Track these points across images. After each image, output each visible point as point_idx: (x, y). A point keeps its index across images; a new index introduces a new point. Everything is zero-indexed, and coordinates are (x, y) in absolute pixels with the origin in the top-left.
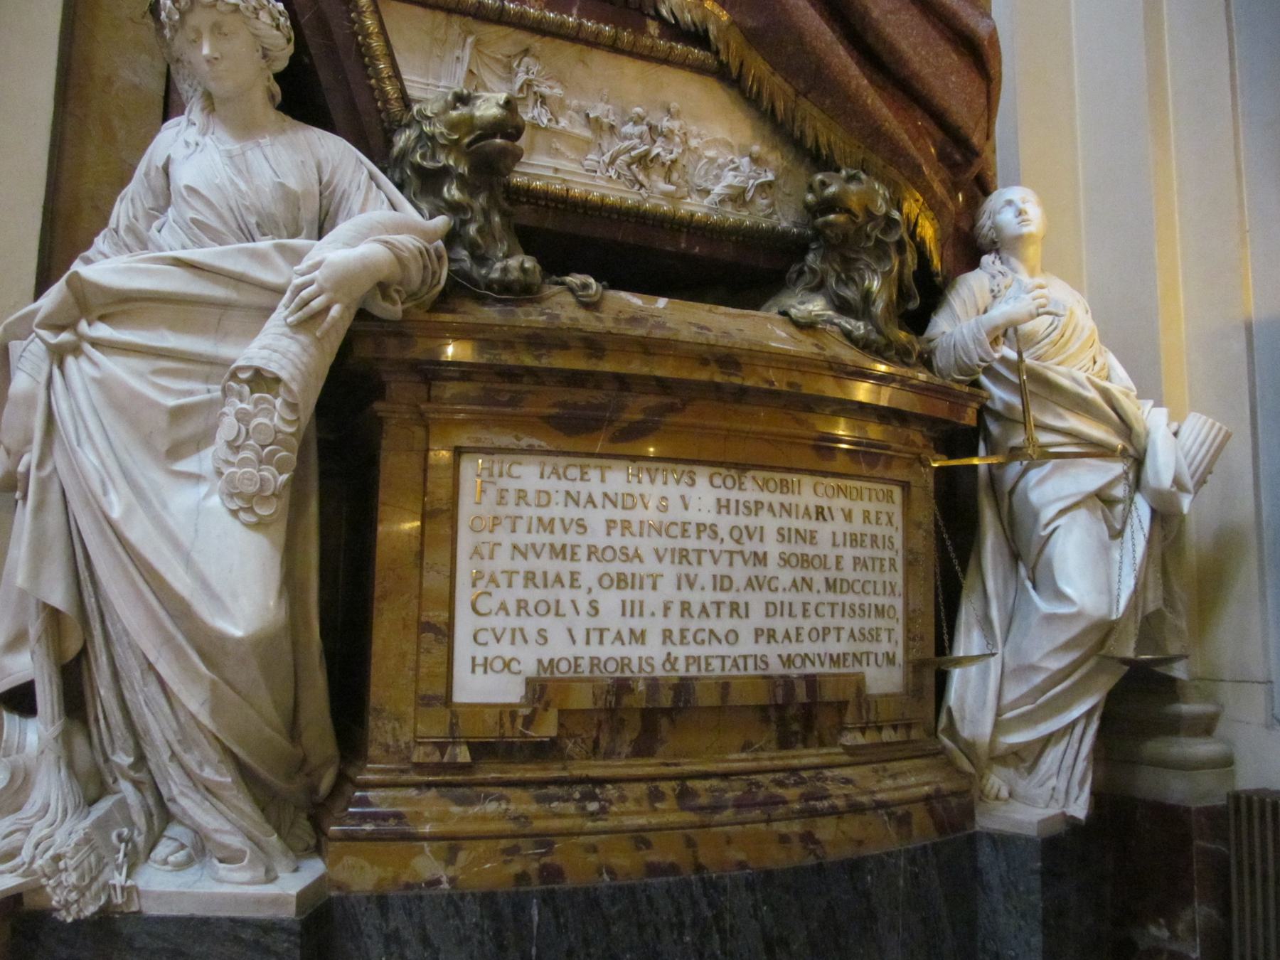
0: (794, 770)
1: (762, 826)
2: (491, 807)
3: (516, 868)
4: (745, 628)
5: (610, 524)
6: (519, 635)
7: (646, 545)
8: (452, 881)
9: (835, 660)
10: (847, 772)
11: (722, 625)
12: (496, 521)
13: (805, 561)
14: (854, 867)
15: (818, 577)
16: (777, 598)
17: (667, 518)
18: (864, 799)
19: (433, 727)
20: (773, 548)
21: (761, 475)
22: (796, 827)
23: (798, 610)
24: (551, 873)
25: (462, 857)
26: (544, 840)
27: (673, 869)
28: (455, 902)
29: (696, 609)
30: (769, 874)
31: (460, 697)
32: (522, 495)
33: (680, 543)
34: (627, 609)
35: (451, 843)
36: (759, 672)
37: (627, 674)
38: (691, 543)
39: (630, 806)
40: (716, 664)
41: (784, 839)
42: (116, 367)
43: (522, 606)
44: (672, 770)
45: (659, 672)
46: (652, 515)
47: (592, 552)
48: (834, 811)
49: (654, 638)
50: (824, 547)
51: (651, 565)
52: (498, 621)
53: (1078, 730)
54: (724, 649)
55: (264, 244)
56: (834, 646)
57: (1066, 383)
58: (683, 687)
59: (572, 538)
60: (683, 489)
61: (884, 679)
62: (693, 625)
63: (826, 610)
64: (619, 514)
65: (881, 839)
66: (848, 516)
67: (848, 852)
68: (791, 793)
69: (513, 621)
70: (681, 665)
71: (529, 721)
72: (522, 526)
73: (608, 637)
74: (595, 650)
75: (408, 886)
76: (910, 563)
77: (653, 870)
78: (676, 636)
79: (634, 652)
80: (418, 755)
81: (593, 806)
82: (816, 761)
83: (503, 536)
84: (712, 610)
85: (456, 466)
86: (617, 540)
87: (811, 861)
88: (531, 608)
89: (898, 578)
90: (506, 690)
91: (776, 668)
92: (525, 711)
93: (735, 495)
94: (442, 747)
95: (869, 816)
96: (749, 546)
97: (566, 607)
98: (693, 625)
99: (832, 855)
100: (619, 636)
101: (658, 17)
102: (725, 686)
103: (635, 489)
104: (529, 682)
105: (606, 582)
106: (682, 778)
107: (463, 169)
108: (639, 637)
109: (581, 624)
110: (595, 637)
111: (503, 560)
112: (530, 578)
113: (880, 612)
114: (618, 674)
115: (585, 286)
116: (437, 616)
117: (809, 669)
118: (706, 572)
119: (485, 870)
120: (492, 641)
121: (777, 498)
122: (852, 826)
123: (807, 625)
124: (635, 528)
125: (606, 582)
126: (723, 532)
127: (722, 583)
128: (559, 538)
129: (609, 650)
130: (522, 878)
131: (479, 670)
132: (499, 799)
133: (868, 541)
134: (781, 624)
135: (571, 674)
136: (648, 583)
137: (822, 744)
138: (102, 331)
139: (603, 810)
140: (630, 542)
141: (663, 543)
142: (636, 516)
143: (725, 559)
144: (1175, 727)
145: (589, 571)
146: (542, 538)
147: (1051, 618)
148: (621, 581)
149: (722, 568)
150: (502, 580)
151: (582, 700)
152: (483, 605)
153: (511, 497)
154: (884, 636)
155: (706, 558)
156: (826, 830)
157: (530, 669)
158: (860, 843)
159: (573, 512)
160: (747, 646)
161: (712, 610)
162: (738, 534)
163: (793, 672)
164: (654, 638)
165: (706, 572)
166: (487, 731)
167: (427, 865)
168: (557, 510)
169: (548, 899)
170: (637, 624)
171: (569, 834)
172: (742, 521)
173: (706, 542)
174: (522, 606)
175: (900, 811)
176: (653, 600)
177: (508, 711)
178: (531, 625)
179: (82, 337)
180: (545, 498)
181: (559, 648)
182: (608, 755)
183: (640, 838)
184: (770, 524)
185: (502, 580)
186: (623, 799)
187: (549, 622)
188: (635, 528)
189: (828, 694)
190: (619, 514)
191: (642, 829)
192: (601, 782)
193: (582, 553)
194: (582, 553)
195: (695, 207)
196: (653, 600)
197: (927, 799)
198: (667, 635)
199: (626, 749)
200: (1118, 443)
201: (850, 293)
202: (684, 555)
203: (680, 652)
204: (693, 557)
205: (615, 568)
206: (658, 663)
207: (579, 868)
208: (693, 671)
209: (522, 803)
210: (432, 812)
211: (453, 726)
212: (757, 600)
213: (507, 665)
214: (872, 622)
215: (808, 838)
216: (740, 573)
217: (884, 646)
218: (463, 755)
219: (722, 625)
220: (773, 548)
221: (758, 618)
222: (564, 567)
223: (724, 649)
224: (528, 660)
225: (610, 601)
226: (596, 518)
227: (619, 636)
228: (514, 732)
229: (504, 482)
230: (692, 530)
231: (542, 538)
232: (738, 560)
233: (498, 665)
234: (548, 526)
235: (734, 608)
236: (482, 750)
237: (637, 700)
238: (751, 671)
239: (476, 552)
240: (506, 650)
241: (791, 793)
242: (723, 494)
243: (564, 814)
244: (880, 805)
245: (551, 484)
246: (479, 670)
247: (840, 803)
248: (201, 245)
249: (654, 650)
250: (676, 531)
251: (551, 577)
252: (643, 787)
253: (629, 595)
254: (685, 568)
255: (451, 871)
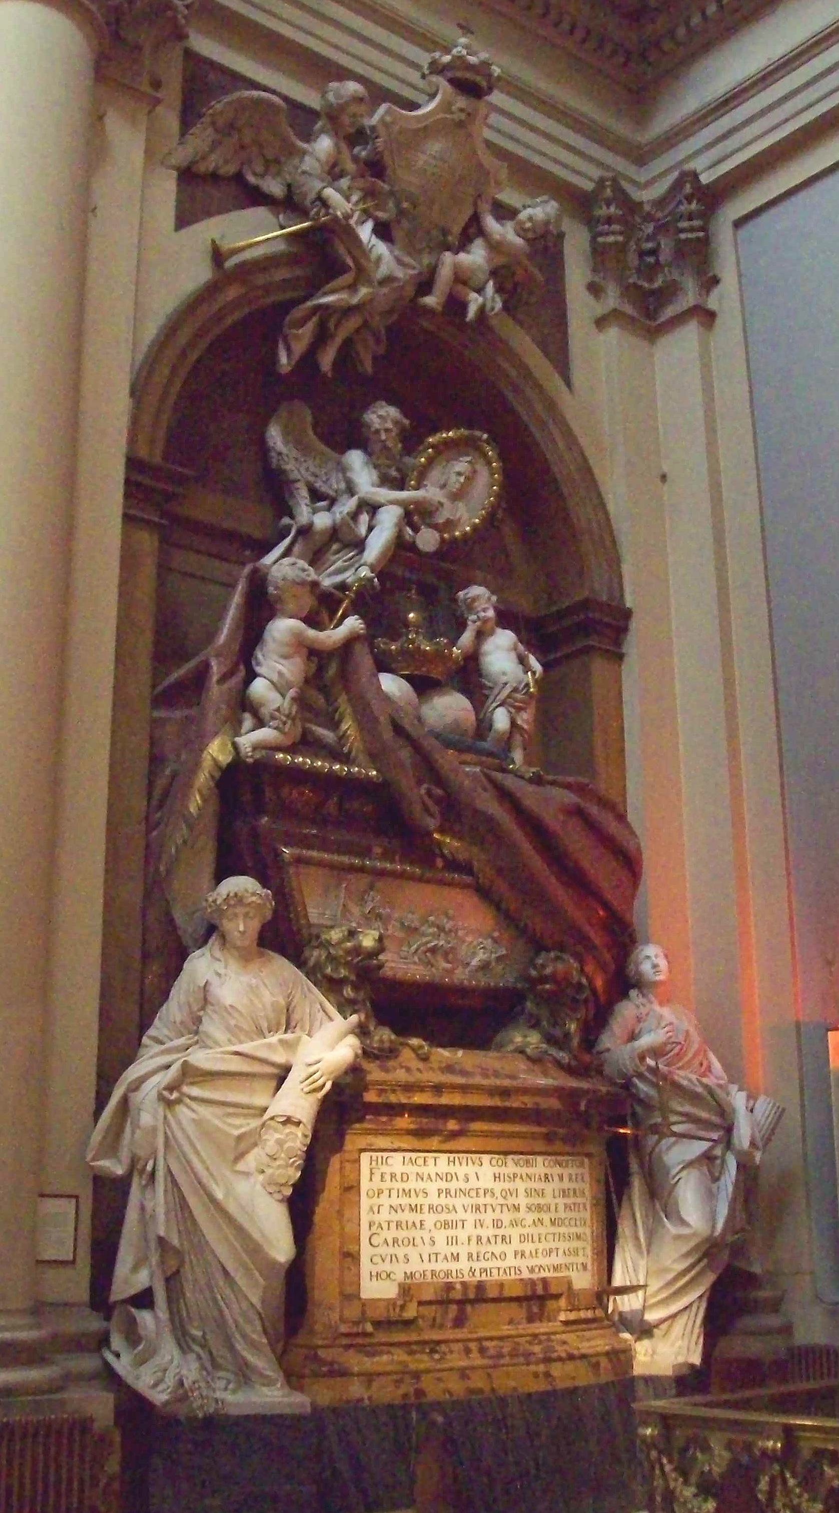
0: (535, 1336)
1: (524, 1368)
2: (385, 1358)
3: (401, 1392)
4: (509, 1250)
5: (440, 1192)
6: (394, 1258)
7: (459, 1202)
8: (370, 1398)
9: (556, 1268)
10: (564, 1337)
11: (498, 1249)
12: (380, 1192)
13: (539, 1208)
14: (574, 1391)
15: (546, 1217)
16: (525, 1231)
17: (468, 1186)
18: (576, 1352)
19: (352, 1312)
20: (523, 1201)
21: (516, 1157)
22: (541, 1368)
23: (536, 1238)
24: (420, 1393)
25: (375, 1385)
26: (417, 1375)
27: (481, 1391)
28: (374, 1411)
29: (484, 1240)
30: (529, 1395)
31: (364, 1295)
32: (393, 1176)
33: (475, 1201)
34: (452, 1241)
35: (369, 1377)
36: (518, 1277)
37: (450, 1280)
38: (481, 1201)
39: (455, 1355)
40: (495, 1272)
41: (536, 1375)
42: (204, 1111)
43: (395, 1241)
44: (475, 1336)
45: (466, 1278)
46: (462, 1185)
47: (431, 1208)
48: (560, 1359)
49: (463, 1257)
50: (548, 1199)
51: (461, 1215)
52: (383, 1250)
53: (694, 1308)
54: (499, 1263)
55: (274, 1039)
56: (555, 1260)
57: (685, 1083)
58: (480, 1287)
59: (420, 1200)
60: (476, 1168)
61: (583, 1280)
62: (483, 1249)
63: (550, 1237)
64: (444, 1185)
65: (583, 1376)
66: (561, 1178)
67: (569, 1384)
68: (537, 1349)
69: (391, 1250)
70: (477, 1273)
71: (403, 1307)
72: (394, 1194)
73: (440, 1257)
74: (433, 1266)
75: (348, 1402)
76: (594, 1205)
77: (471, 1391)
78: (475, 1256)
79: (453, 1266)
80: (344, 1329)
81: (437, 1356)
82: (547, 1330)
83: (384, 1200)
84: (493, 1240)
85: (358, 1161)
86: (443, 1200)
87: (549, 1388)
88: (400, 1242)
89: (587, 1215)
90: (388, 1291)
91: (526, 1275)
92: (400, 1303)
93: (503, 1170)
94: (356, 1323)
95: (578, 1363)
96: (511, 1201)
97: (418, 1241)
98: (483, 1249)
99: (560, 1385)
100: (446, 1258)
101: (443, 856)
102: (501, 1285)
103: (452, 1169)
104: (399, 1285)
105: (438, 1225)
106: (479, 1340)
107: (353, 977)
108: (456, 1258)
109: (426, 1250)
110: (433, 1258)
111: (385, 1215)
112: (398, 1225)
113: (578, 1237)
114: (446, 1280)
115: (421, 1047)
116: (352, 1248)
117: (543, 1274)
118: (488, 1217)
119: (386, 1393)
120: (380, 1261)
121: (524, 1170)
122: (570, 1367)
123: (541, 1247)
124: (453, 1193)
125: (438, 1225)
126: (498, 1194)
127: (497, 1224)
128: (413, 1201)
129: (441, 1266)
130: (405, 1396)
131: (374, 1279)
132: (389, 1352)
133: (572, 1193)
134: (528, 1247)
135: (422, 1280)
136: (460, 1224)
137: (549, 1321)
138: (195, 1091)
139: (442, 1359)
140: (450, 1201)
141: (467, 1201)
142: (453, 1185)
143: (498, 1209)
144: (754, 1308)
145: (430, 1219)
146: (404, 1201)
147: (678, 1237)
148: (446, 1225)
149: (497, 1215)
150: (385, 1226)
151: (428, 1295)
152: (375, 1241)
153: (387, 1177)
154: (581, 1253)
155: (489, 1209)
156: (557, 1370)
157: (400, 1277)
158: (574, 1378)
159: (421, 1185)
160: (511, 1261)
161: (493, 1240)
162: (506, 1193)
163: (534, 1276)
164: (463, 1257)
165: (488, 1217)
166: (380, 1313)
167: (356, 1389)
168: (412, 1184)
169: (419, 1407)
170: (454, 1249)
171: (428, 1371)
172: (507, 1185)
173: (488, 1200)
174: (395, 1241)
175: (594, 1360)
176: (462, 1235)
177: (391, 1303)
178: (400, 1252)
179: (183, 1094)
180: (405, 1177)
181: (415, 1266)
182: (442, 1326)
183: (463, 1374)
184: (521, 1186)
185: (385, 1226)
186: (451, 1352)
187: (409, 1250)
188: (453, 1193)
189: (553, 1290)
190: (444, 1185)
191: (466, 1368)
192: (439, 1342)
193: (426, 1209)
194: (426, 1209)
195: (461, 976)
196: (462, 1235)
197: (607, 1354)
198: (470, 1256)
199: (449, 1324)
200: (715, 1119)
201: (558, 1032)
202: (478, 1208)
203: (477, 1266)
204: (482, 1209)
205: (444, 1217)
206: (466, 1273)
207: (434, 1391)
208: (484, 1277)
209: (400, 1355)
210: (357, 1362)
211: (363, 1313)
212: (515, 1233)
213: (389, 1276)
214: (575, 1244)
215: (547, 1375)
216: (507, 1217)
217: (580, 1259)
218: (369, 1328)
219: (498, 1249)
220: (523, 1201)
221: (516, 1245)
222: (416, 1217)
223: (499, 1263)
224: (399, 1272)
225: (441, 1236)
226: (432, 1187)
227: (446, 1258)
228: (394, 1315)
229: (384, 1169)
230: (481, 1192)
231: (404, 1201)
232: (505, 1208)
233: (384, 1276)
234: (407, 1193)
235: (503, 1238)
236: (377, 1324)
237: (457, 1295)
238: (513, 1276)
239: (371, 1209)
240: (387, 1267)
241: (537, 1349)
242: (497, 1170)
243: (422, 1362)
244: (583, 1357)
245: (411, 1169)
246: (374, 1279)
247: (564, 1355)
248: (241, 1042)
249: (464, 1265)
250: (473, 1193)
251: (410, 1224)
252: (460, 1345)
253: (451, 1232)
254: (478, 1216)
255: (369, 1394)
